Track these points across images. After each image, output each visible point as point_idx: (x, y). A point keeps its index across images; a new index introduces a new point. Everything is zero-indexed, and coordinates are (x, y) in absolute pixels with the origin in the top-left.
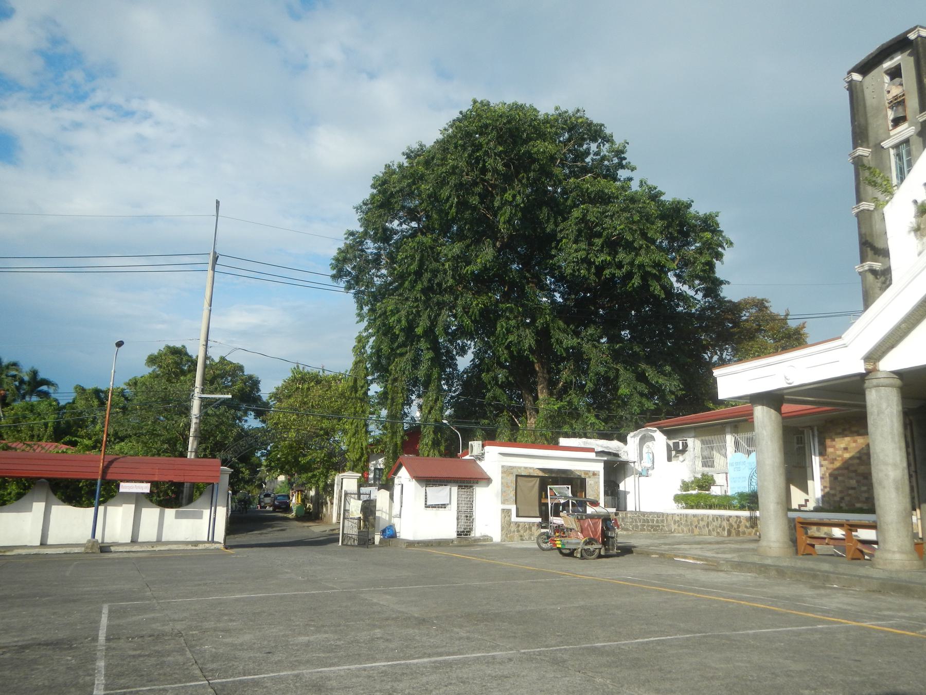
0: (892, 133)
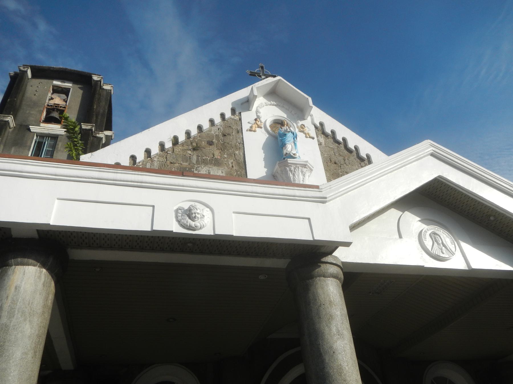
0: (42, 125)
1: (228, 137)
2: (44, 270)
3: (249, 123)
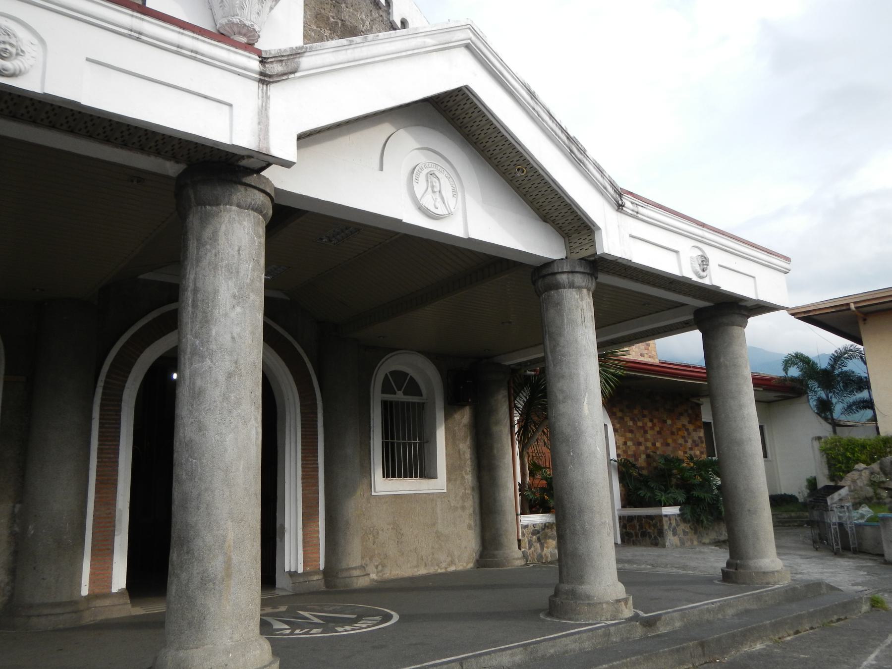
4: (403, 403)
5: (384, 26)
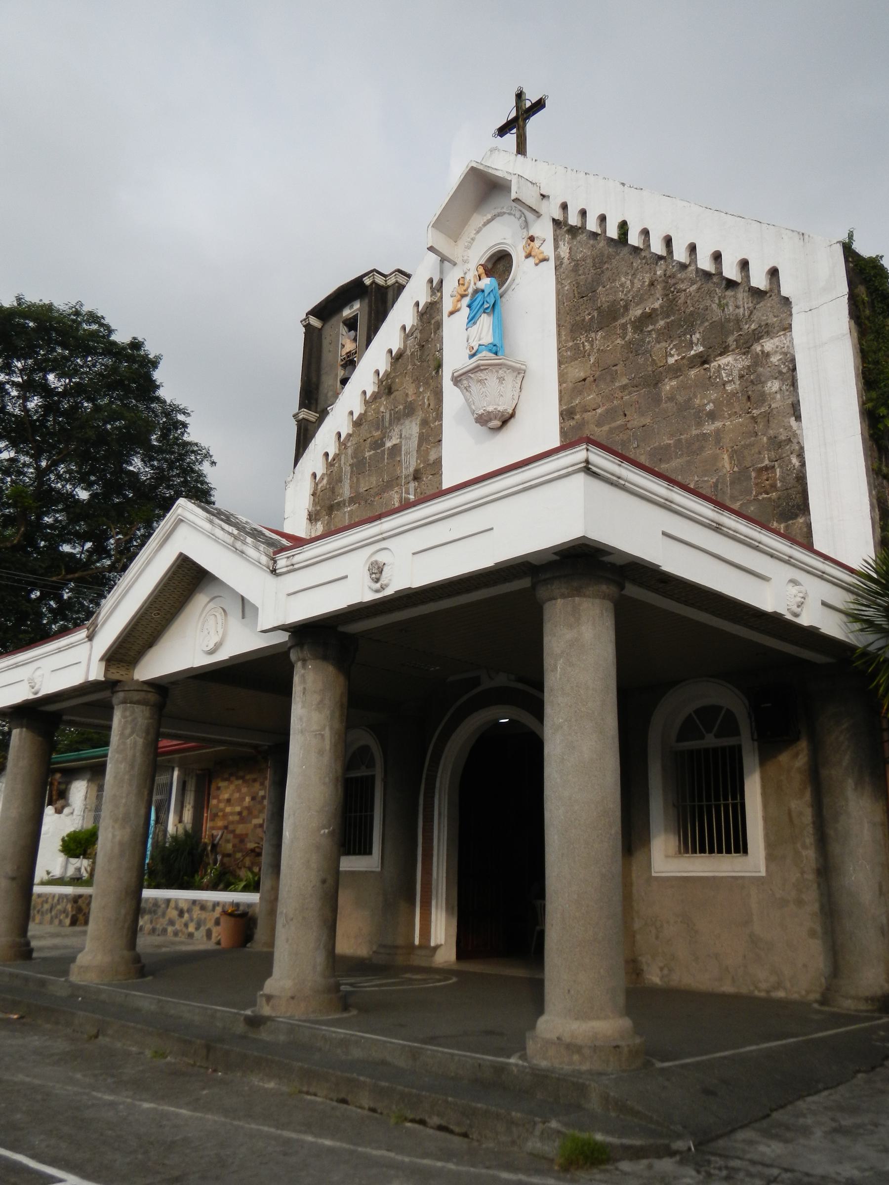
1: (426, 347)
2: (24, 729)
3: (452, 297)
4: (715, 750)
5: (648, 267)
